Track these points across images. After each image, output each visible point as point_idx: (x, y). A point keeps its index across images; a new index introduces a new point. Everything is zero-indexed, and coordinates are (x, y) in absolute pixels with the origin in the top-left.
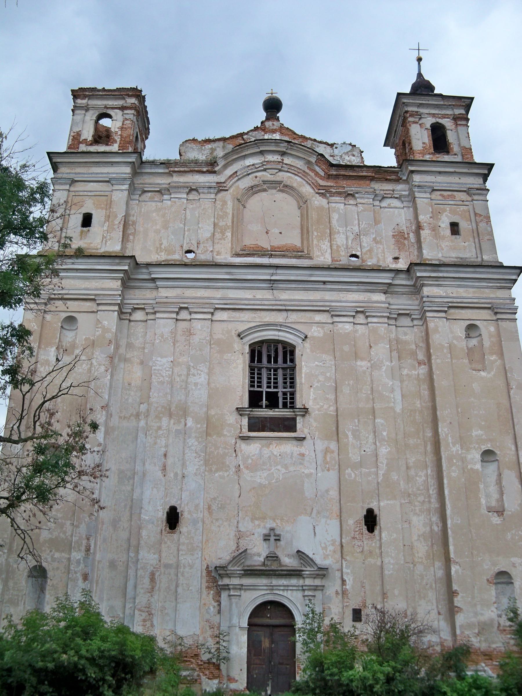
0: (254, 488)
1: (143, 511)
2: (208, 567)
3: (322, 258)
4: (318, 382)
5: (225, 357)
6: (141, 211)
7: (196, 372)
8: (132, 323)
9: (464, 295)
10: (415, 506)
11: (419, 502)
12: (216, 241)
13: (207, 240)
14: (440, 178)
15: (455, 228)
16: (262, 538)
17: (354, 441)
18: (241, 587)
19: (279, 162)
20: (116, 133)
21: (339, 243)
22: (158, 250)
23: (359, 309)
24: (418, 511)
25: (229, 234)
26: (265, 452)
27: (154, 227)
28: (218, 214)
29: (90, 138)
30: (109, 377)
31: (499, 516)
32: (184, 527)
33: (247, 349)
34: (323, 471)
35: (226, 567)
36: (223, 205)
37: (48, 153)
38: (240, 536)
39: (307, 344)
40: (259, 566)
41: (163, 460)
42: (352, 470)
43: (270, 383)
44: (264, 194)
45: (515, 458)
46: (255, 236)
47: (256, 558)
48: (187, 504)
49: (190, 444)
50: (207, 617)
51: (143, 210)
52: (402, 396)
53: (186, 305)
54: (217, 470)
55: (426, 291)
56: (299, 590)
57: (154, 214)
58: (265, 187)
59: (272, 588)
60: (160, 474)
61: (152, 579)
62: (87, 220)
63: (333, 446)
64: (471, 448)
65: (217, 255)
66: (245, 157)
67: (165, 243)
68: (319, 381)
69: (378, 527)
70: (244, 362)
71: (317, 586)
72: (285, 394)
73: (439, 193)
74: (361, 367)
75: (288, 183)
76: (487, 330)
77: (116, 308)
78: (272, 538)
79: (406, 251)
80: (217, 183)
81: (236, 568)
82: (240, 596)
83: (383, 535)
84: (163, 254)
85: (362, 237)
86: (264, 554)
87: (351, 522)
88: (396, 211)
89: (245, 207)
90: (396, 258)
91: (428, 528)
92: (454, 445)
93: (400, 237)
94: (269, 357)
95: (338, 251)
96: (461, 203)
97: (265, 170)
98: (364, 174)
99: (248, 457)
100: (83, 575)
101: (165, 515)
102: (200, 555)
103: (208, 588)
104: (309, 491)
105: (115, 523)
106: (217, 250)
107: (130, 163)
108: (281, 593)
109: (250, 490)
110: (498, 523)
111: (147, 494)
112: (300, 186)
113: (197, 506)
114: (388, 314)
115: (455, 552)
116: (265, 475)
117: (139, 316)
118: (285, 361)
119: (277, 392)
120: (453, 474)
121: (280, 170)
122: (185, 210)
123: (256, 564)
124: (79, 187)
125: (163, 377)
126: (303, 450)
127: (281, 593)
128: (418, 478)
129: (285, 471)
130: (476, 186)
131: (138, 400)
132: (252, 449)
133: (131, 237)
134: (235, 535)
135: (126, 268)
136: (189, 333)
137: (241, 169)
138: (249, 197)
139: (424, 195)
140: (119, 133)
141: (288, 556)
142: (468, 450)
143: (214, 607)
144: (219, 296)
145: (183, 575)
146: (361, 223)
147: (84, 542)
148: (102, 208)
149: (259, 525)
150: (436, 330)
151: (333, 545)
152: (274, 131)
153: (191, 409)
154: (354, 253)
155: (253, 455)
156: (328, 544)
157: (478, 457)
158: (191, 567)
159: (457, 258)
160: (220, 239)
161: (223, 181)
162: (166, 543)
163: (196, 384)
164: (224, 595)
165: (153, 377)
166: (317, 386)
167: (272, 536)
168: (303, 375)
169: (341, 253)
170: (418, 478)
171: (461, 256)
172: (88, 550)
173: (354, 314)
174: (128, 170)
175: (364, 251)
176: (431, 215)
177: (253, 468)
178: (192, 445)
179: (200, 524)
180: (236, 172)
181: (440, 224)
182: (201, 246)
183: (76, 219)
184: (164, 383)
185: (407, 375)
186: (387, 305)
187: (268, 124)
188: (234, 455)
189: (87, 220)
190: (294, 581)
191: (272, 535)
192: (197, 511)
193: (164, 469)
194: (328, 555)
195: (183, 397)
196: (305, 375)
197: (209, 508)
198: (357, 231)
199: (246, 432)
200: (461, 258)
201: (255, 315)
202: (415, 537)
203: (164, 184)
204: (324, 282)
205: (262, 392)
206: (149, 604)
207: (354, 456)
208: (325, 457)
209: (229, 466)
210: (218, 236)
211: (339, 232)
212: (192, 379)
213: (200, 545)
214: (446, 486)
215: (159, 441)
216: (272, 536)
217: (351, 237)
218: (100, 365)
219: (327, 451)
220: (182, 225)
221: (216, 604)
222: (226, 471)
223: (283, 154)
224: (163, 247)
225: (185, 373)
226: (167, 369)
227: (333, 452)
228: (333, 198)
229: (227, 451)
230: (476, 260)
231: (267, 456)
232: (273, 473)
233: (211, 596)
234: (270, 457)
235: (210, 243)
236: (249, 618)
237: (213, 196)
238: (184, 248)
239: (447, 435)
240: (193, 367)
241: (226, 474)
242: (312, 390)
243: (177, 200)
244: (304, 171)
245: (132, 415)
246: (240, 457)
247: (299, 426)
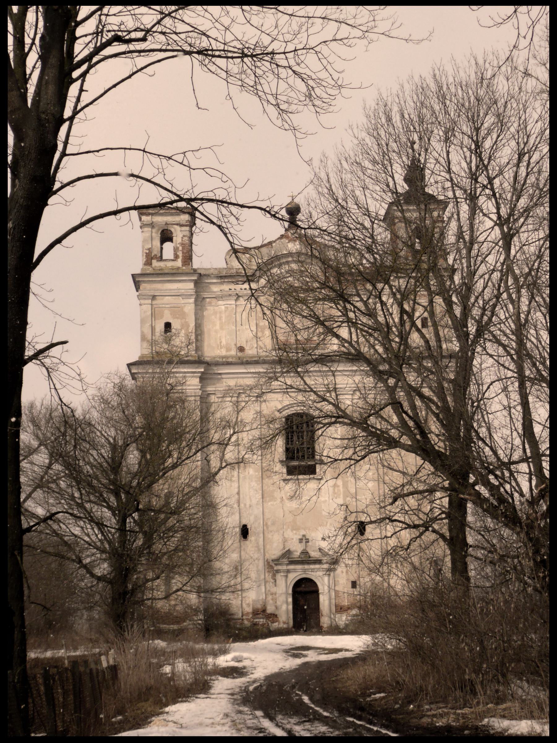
16: (298, 541)
32: (251, 537)
38: (285, 541)
41: (237, 496)
59: (305, 571)
67: (224, 342)
78: (304, 541)
135: (202, 370)
140: (181, 248)
148: (177, 318)
167: (304, 540)
174: (191, 285)
179: (262, 535)
182: (249, 343)
190: (317, 566)
197: (266, 524)
208: (334, 490)
220: (234, 328)
227: (338, 486)
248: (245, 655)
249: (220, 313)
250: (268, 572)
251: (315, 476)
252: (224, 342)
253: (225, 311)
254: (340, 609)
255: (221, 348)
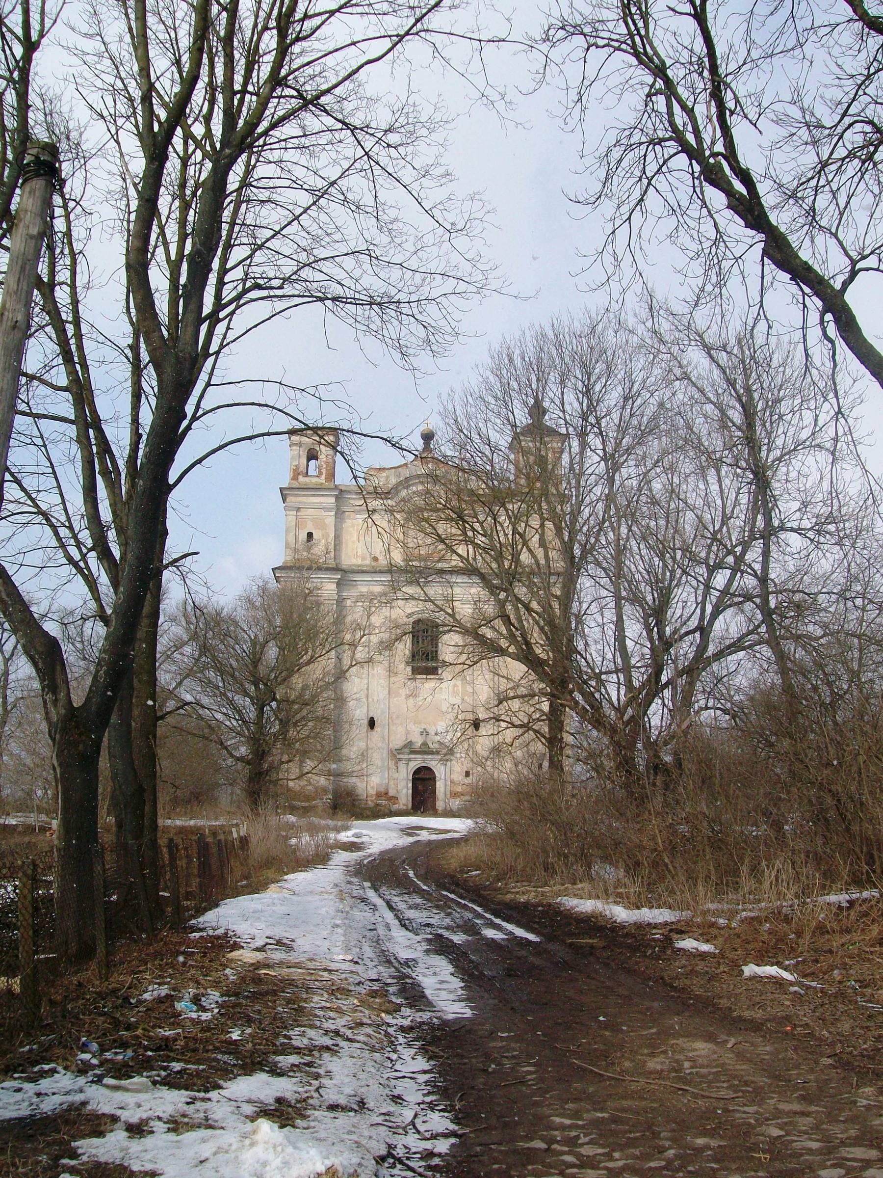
32: (377, 728)
38: (408, 733)
59: (424, 760)
67: (360, 553)
167: (425, 733)
174: (333, 500)
216: (425, 733)
248: (365, 832)
252: (360, 553)
254: (454, 795)
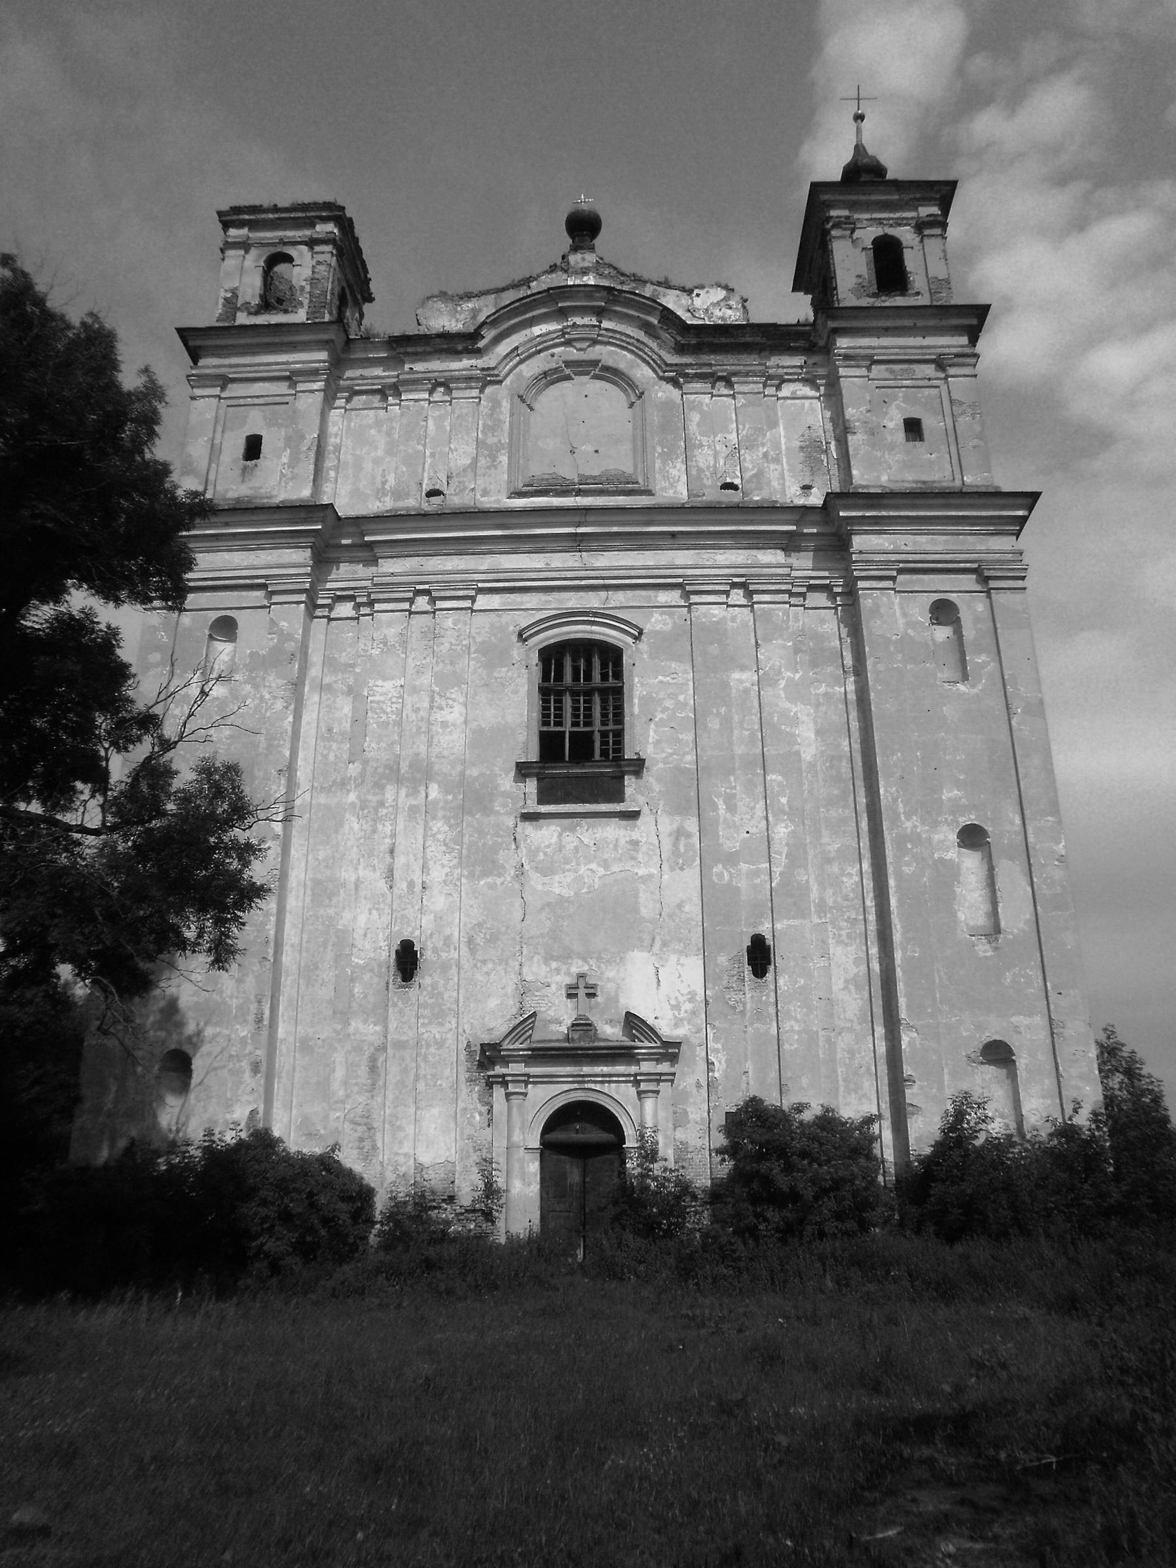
0: (548, 904)
1: (355, 950)
2: (469, 1045)
3: (671, 492)
4: (663, 712)
5: (495, 674)
6: (349, 426)
7: (444, 703)
8: (334, 623)
9: (929, 548)
10: (840, 929)
11: (847, 921)
12: (479, 472)
13: (464, 470)
14: (885, 341)
15: (913, 428)
16: (564, 992)
17: (728, 815)
18: (527, 1080)
19: (594, 326)
20: (302, 288)
21: (701, 465)
22: (380, 493)
23: (736, 580)
24: (844, 937)
25: (504, 459)
26: (569, 839)
27: (373, 454)
28: (484, 425)
29: (256, 301)
30: (291, 719)
31: (989, 942)
32: (425, 978)
33: (535, 658)
34: (672, 869)
35: (499, 1044)
36: (493, 409)
37: (180, 331)
38: (524, 990)
39: (643, 646)
40: (558, 1041)
41: (388, 859)
42: (724, 867)
43: (578, 716)
44: (566, 384)
45: (1021, 838)
46: (550, 458)
47: (554, 1027)
48: (431, 934)
49: (435, 829)
50: (469, 1131)
51: (353, 424)
52: (818, 732)
53: (427, 587)
54: (484, 874)
55: (858, 542)
56: (629, 1082)
57: (373, 432)
58: (568, 371)
60: (382, 885)
61: (373, 1069)
62: (253, 448)
63: (692, 825)
64: (940, 822)
65: (482, 496)
66: (531, 322)
67: (391, 480)
68: (665, 709)
69: (772, 967)
70: (530, 682)
71: (661, 1074)
72: (604, 734)
73: (883, 367)
74: (741, 681)
75: (610, 363)
76: (972, 609)
77: (303, 597)
78: (582, 992)
79: (824, 474)
80: (483, 369)
81: (517, 1045)
82: (525, 1094)
83: (781, 982)
84: (388, 499)
85: (742, 452)
86: (569, 1022)
87: (723, 960)
88: (807, 403)
89: (532, 409)
90: (807, 488)
91: (864, 968)
92: (908, 818)
93: (811, 450)
94: (576, 670)
95: (699, 478)
96: (926, 383)
97: (568, 343)
98: (749, 339)
99: (538, 850)
100: (251, 1064)
101: (393, 956)
102: (454, 1025)
103: (470, 1080)
104: (647, 909)
105: (308, 973)
106: (482, 486)
107: (327, 342)
108: (598, 1087)
109: (543, 908)
110: (988, 954)
111: (362, 919)
112: (632, 367)
113: (447, 940)
114: (789, 587)
115: (909, 1007)
116: (569, 880)
117: (345, 609)
118: (604, 677)
119: (593, 732)
120: (906, 869)
121: (595, 342)
122: (426, 419)
123: (554, 1038)
124: (235, 390)
125: (385, 713)
126: (635, 835)
127: (598, 1087)
128: (845, 879)
129: (604, 872)
130: (954, 350)
131: (345, 756)
132: (546, 835)
133: (332, 474)
134: (517, 989)
136: (433, 635)
137: (526, 343)
138: (540, 392)
139: (857, 372)
140: (308, 288)
141: (611, 1022)
142: (935, 825)
143: (481, 1114)
144: (483, 568)
145: (425, 1059)
146: (741, 427)
147: (253, 1007)
149: (558, 970)
150: (876, 611)
151: (690, 1001)
152: (584, 272)
153: (436, 768)
154: (729, 480)
155: (548, 846)
156: (682, 999)
157: (953, 837)
158: (440, 1044)
159: (917, 482)
160: (489, 468)
161: (492, 365)
162: (395, 1005)
163: (444, 724)
164: (498, 1092)
165: (370, 714)
166: (661, 719)
167: (581, 990)
168: (636, 701)
169: (705, 481)
170: (845, 879)
171: (924, 478)
172: (259, 1020)
173: (727, 588)
175: (747, 476)
176: (868, 407)
177: (547, 871)
178: (439, 832)
179: (454, 971)
180: (517, 348)
181: (886, 422)
182: (454, 482)
183: (235, 445)
184: (388, 724)
185: (826, 694)
186: (786, 571)
187: (575, 259)
188: (513, 847)
189: (253, 448)
190: (620, 1069)
191: (581, 985)
192: (448, 947)
193: (390, 875)
194: (682, 1020)
195: (423, 749)
196: (641, 698)
198: (736, 441)
199: (533, 806)
200: (924, 482)
201: (550, 598)
202: (841, 984)
203: (388, 377)
204: (673, 535)
205: (564, 732)
206: (369, 1111)
207: (731, 842)
209: (503, 867)
210: (483, 462)
211: (701, 445)
212: (439, 716)
213: (455, 1006)
214: (892, 891)
215: (380, 827)
216: (581, 990)
217: (724, 451)
218: (275, 698)
219: (680, 833)
220: (420, 448)
221: (484, 1109)
222: (499, 875)
223: (600, 313)
224: (387, 487)
225: (426, 704)
226: (394, 700)
227: (689, 835)
228: (691, 385)
229: (500, 840)
230: (951, 484)
231: (571, 846)
232: (582, 877)
233: (475, 1096)
234: (576, 848)
235: (470, 474)
236: (544, 1133)
237: (475, 393)
238: (424, 486)
239: (895, 800)
240: (439, 694)
241: (499, 881)
242: (652, 726)
243: (412, 403)
244: (638, 340)
245: (334, 782)
246: (523, 850)
247: (628, 791)
249: (391, 419)
250: (470, 1080)
251: (618, 807)
252: (391, 480)
253: (402, 414)
255: (385, 495)
